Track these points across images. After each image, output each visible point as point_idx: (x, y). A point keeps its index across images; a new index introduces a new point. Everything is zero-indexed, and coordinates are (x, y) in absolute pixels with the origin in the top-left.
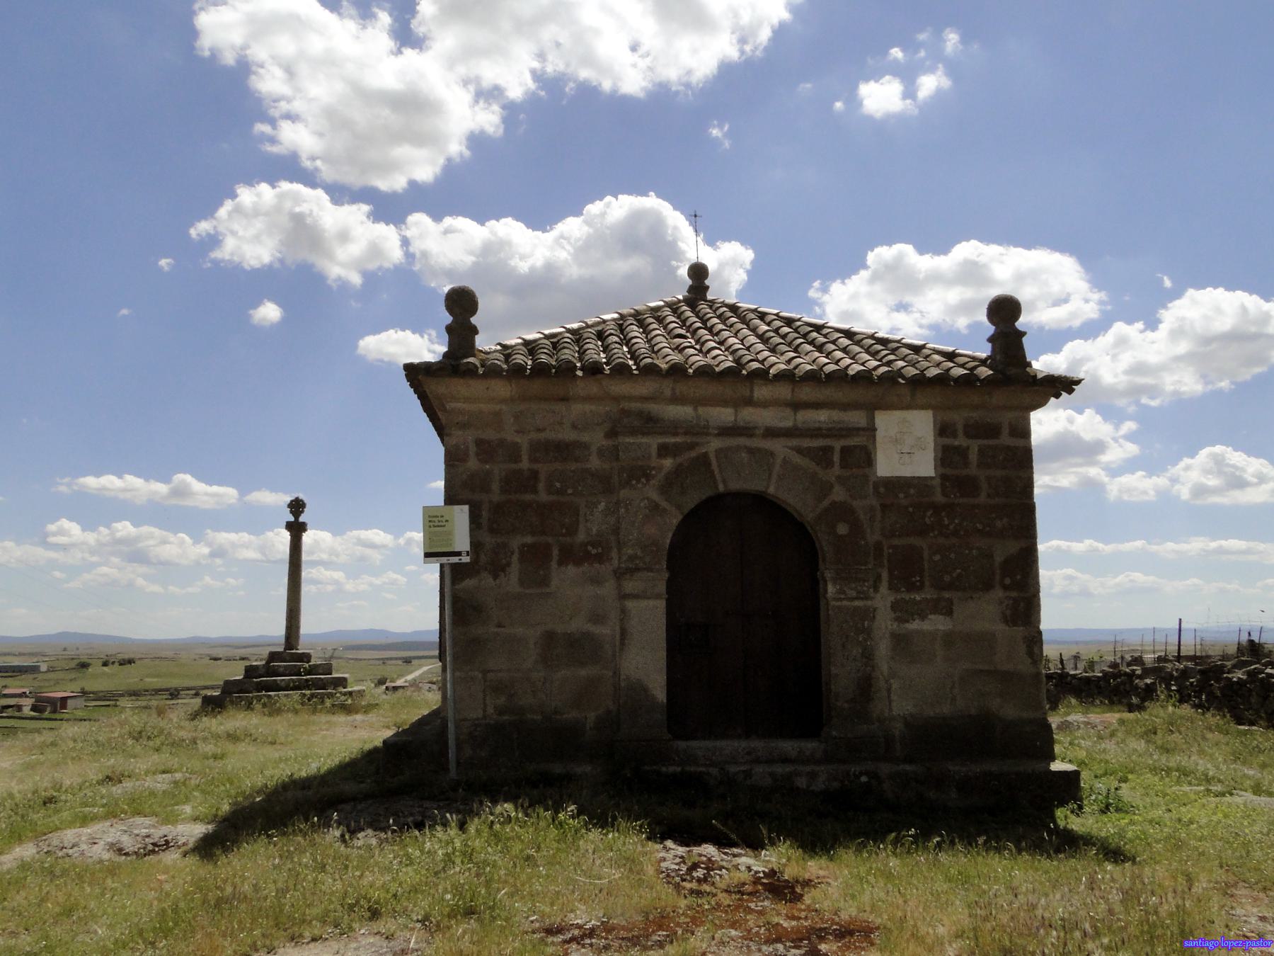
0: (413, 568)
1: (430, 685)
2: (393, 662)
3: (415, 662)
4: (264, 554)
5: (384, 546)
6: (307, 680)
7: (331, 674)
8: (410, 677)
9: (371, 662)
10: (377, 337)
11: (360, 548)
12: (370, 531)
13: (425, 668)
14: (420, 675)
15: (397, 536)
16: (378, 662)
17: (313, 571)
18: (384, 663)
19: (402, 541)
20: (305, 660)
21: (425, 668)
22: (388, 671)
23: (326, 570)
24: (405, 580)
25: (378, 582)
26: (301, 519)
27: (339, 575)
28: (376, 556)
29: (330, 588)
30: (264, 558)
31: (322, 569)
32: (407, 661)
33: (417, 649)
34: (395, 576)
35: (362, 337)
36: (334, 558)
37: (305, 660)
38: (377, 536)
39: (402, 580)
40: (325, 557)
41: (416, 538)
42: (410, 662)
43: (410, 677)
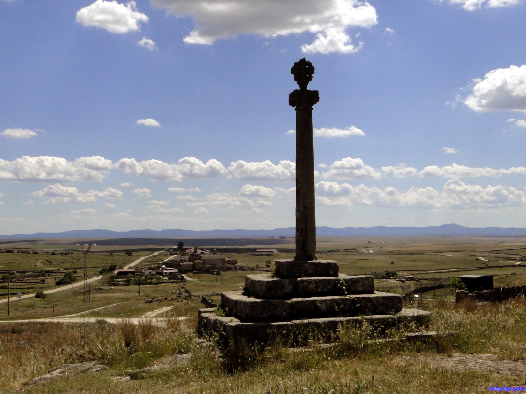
0: (127, 184)
1: (150, 271)
2: (118, 254)
3: (134, 254)
4: (16, 174)
5: (105, 168)
6: (353, 300)
7: (372, 292)
8: (132, 265)
9: (104, 254)
10: (88, 8)
11: (87, 169)
12: (93, 157)
13: (143, 258)
14: (139, 263)
15: (114, 162)
16: (122, 254)
17: (53, 187)
18: (111, 254)
19: (117, 165)
20: (332, 272)
21: (143, 258)
22: (116, 259)
23: (62, 185)
24: (122, 193)
25: (101, 194)
26: (311, 87)
27: (72, 190)
28: (99, 176)
29: (66, 199)
30: (16, 178)
31: (60, 186)
32: (129, 253)
33: (146, 244)
34: (113, 190)
35: (79, 9)
36: (68, 178)
37: (332, 272)
38: (100, 161)
39: (119, 193)
40: (61, 176)
41: (128, 163)
42: (131, 254)
43: (132, 265)
